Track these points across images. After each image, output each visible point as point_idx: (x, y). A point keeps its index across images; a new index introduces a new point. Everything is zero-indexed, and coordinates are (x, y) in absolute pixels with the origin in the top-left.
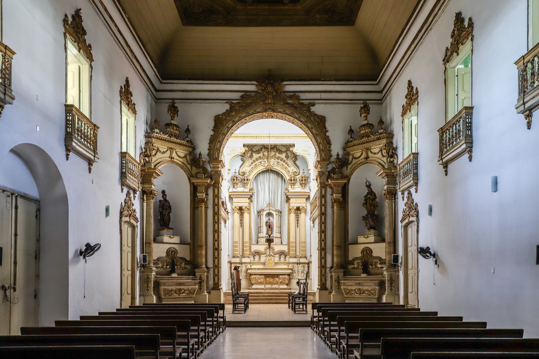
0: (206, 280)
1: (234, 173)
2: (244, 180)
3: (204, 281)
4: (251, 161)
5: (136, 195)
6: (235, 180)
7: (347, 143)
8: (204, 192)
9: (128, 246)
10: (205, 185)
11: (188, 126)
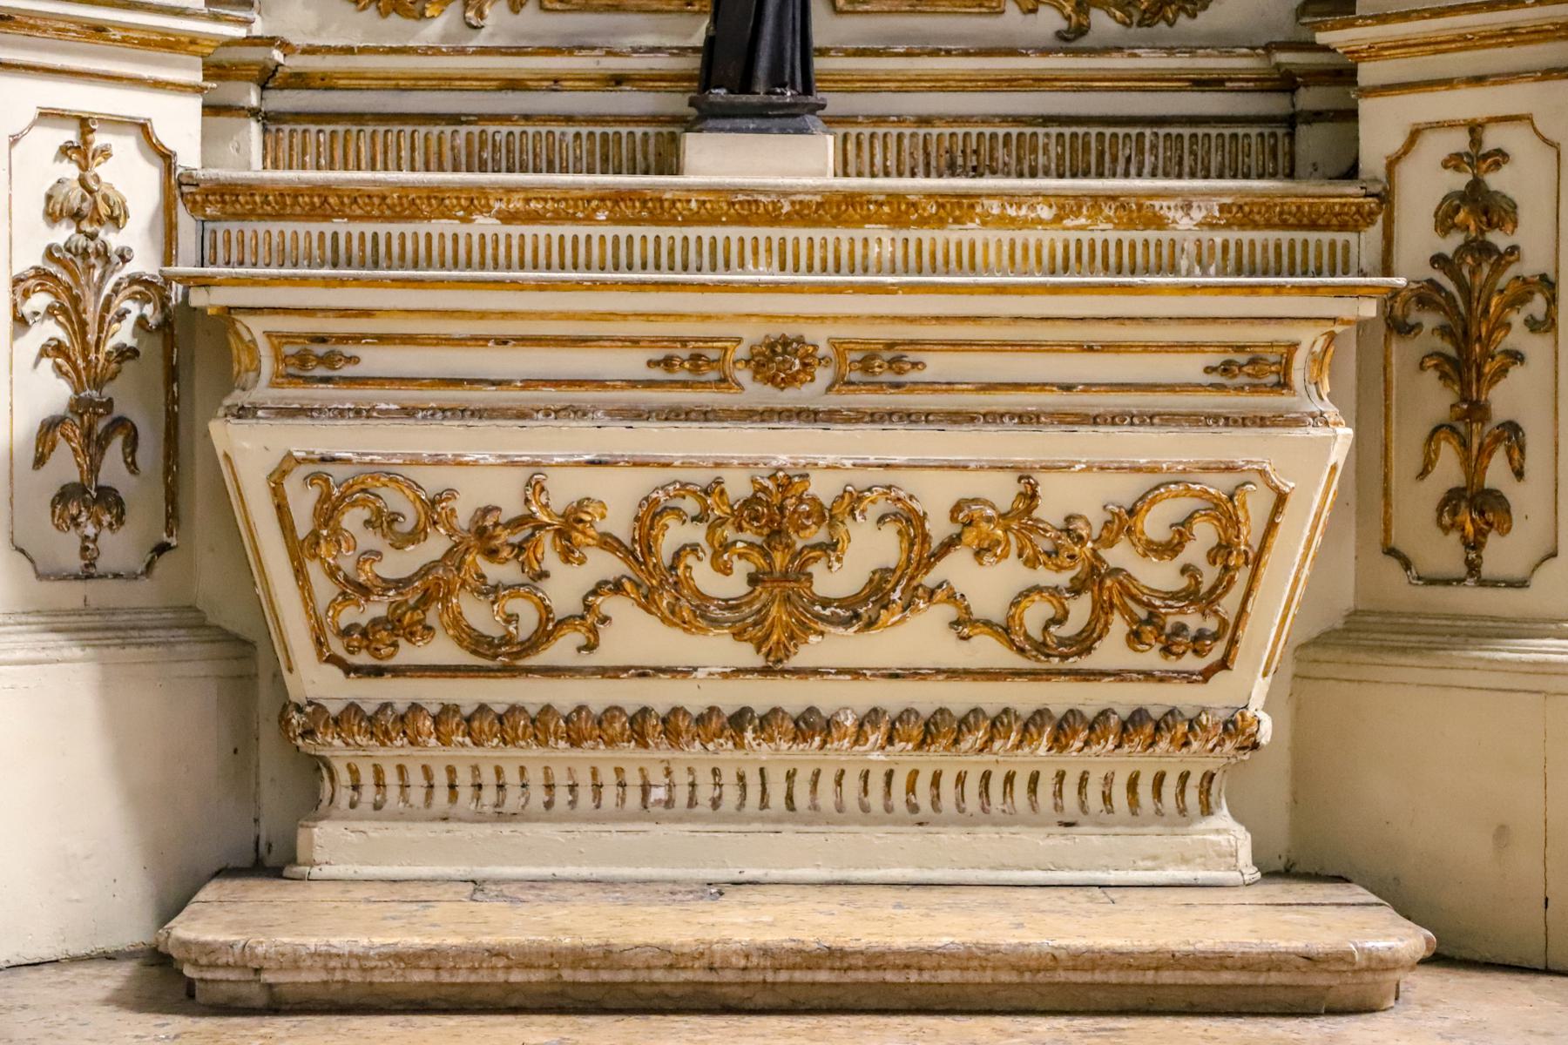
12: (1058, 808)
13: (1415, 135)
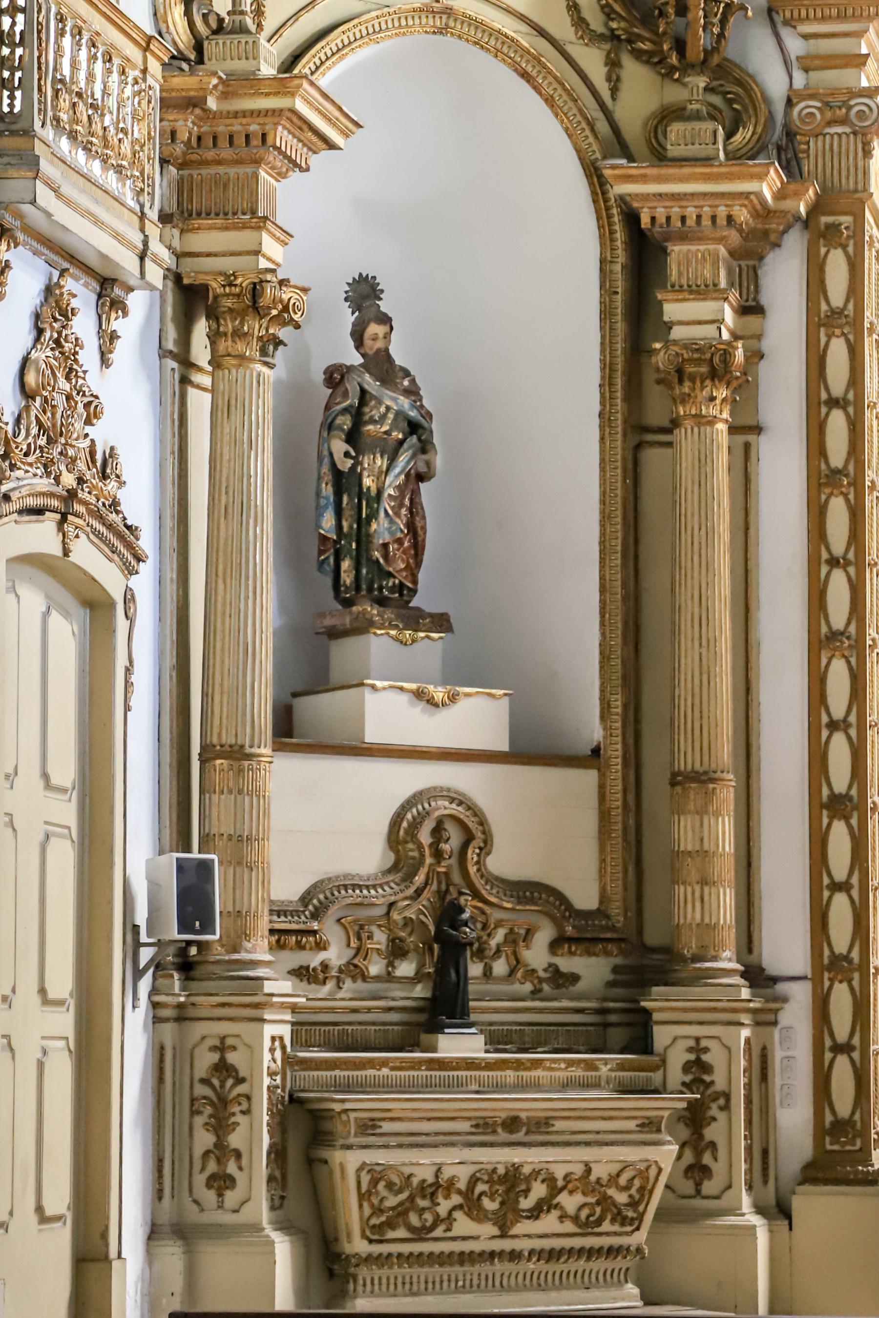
0: (748, 1086)
3: (727, 1096)
5: (117, 324)
8: (723, 284)
9: (45, 776)
10: (730, 219)
12: (583, 1282)
13: (675, 1039)
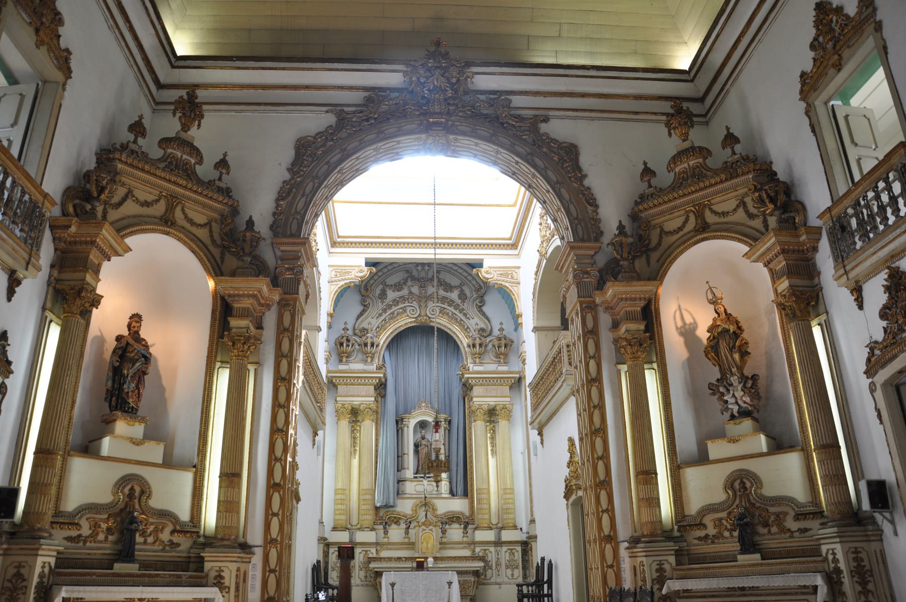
1: (343, 329)
2: (366, 345)
3: (229, 588)
4: (381, 306)
6: (345, 345)
7: (639, 200)
11: (225, 155)
